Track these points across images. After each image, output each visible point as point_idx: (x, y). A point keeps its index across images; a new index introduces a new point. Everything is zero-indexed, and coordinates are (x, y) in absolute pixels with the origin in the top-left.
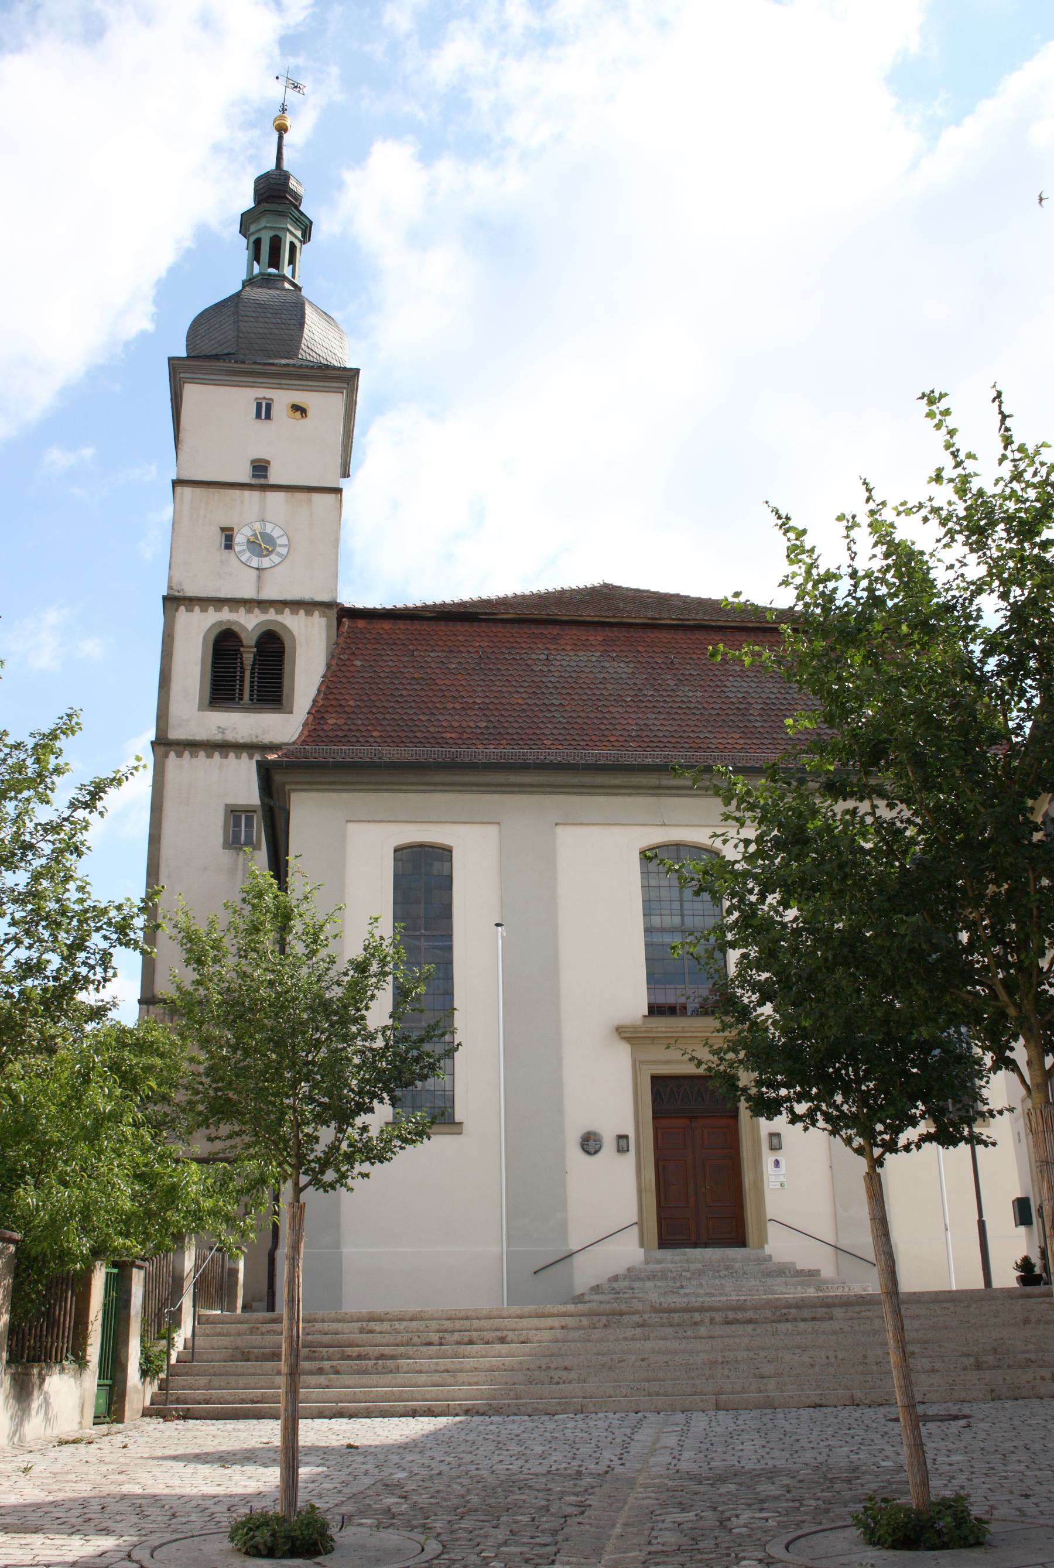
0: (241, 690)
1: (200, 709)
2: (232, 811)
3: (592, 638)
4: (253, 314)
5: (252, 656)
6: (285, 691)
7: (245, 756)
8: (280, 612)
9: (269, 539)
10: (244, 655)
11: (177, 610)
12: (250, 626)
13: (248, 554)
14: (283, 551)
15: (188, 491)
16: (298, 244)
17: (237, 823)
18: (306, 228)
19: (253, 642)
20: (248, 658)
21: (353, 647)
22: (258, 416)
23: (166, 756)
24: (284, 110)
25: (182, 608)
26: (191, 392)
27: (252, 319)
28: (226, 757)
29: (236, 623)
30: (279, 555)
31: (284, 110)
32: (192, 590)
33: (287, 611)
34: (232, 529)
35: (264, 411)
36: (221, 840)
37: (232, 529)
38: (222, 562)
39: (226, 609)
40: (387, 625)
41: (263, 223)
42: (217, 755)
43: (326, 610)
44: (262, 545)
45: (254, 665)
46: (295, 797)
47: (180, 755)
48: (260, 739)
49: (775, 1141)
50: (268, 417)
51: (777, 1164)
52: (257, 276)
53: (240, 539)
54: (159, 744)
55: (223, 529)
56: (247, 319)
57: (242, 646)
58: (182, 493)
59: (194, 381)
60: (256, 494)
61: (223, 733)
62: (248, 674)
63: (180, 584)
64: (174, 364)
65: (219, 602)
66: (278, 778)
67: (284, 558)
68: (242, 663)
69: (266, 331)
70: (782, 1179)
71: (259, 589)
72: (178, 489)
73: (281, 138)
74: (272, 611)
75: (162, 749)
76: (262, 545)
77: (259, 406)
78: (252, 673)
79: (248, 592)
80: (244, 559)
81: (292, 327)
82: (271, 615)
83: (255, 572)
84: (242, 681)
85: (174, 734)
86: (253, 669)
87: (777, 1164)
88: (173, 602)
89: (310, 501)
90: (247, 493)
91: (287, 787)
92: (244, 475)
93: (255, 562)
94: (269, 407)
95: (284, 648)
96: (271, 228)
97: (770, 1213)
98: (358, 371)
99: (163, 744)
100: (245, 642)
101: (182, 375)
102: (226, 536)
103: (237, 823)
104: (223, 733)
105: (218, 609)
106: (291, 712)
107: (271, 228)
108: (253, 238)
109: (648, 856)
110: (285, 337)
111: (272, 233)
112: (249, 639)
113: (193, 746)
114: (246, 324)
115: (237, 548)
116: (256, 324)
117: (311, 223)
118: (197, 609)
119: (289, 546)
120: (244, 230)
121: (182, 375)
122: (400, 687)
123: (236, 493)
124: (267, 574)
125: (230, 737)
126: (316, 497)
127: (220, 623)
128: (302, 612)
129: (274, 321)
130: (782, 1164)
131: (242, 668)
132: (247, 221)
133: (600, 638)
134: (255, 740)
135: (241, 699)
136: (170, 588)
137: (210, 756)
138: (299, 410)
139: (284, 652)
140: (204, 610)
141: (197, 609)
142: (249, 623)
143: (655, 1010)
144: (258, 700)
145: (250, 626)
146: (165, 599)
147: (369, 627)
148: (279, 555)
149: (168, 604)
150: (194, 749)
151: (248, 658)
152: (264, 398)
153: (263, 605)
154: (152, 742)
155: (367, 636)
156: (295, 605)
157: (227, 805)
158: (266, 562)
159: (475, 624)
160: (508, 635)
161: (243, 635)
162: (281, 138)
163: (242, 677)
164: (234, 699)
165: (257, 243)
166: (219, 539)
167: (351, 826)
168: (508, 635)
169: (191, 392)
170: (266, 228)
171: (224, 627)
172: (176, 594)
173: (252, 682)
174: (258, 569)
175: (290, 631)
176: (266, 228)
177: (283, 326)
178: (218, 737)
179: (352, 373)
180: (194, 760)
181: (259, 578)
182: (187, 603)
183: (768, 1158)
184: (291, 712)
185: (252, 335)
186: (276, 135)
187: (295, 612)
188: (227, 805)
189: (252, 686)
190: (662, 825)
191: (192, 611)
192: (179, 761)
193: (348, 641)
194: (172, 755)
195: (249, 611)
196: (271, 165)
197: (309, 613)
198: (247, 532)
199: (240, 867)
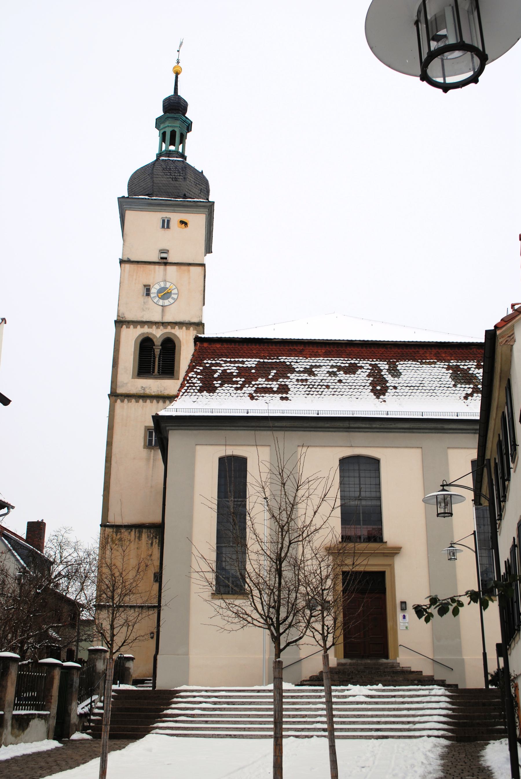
1: (133, 378)
2: (148, 429)
3: (319, 351)
4: (161, 174)
5: (159, 350)
7: (155, 401)
10: (155, 350)
11: (122, 327)
12: (158, 336)
14: (175, 296)
15: (127, 266)
16: (184, 133)
18: (189, 125)
19: (160, 344)
20: (157, 351)
21: (201, 356)
22: (163, 227)
23: (116, 401)
24: (178, 62)
25: (124, 326)
26: (130, 215)
27: (160, 176)
28: (146, 402)
29: (151, 334)
30: (173, 298)
31: (178, 62)
32: (129, 317)
33: (177, 327)
34: (150, 286)
35: (166, 224)
36: (142, 444)
37: (150, 286)
38: (144, 303)
39: (146, 327)
40: (218, 346)
41: (167, 124)
42: (141, 401)
43: (197, 327)
44: (165, 294)
46: (170, 432)
47: (122, 401)
48: (162, 393)
49: (403, 605)
50: (168, 227)
51: (404, 617)
53: (154, 291)
54: (112, 396)
55: (145, 286)
56: (157, 176)
57: (154, 345)
58: (125, 267)
59: (130, 209)
60: (162, 267)
61: (144, 390)
62: (157, 359)
63: (123, 314)
64: (122, 201)
65: (143, 323)
66: (163, 425)
67: (175, 300)
70: (407, 625)
71: (163, 316)
72: (123, 265)
74: (169, 327)
75: (114, 398)
76: (165, 294)
77: (163, 221)
79: (157, 318)
80: (155, 301)
81: (181, 180)
82: (169, 330)
83: (161, 308)
84: (154, 363)
85: (120, 391)
86: (159, 357)
87: (404, 617)
88: (120, 323)
89: (189, 271)
90: (157, 267)
91: (167, 428)
92: (155, 258)
93: (161, 302)
94: (168, 221)
96: (171, 126)
97: (400, 642)
98: (214, 202)
99: (114, 395)
100: (155, 343)
101: (125, 206)
102: (147, 289)
103: (151, 435)
104: (144, 390)
105: (142, 327)
107: (171, 126)
108: (162, 131)
109: (344, 462)
110: (177, 185)
111: (171, 129)
112: (158, 342)
113: (129, 396)
114: (157, 179)
115: (152, 295)
116: (162, 179)
117: (192, 122)
118: (132, 326)
119: (178, 294)
120: (157, 126)
121: (125, 206)
122: (224, 377)
123: (152, 267)
124: (167, 309)
125: (148, 392)
126: (192, 268)
127: (143, 334)
128: (184, 328)
130: (407, 617)
132: (159, 122)
133: (324, 351)
134: (160, 393)
135: (154, 372)
136: (118, 316)
137: (137, 402)
138: (183, 223)
139: (175, 348)
140: (135, 327)
141: (132, 326)
143: (345, 538)
144: (162, 373)
145: (158, 336)
146: (116, 322)
147: (209, 346)
148: (173, 298)
149: (117, 324)
150: (130, 398)
151: (157, 351)
152: (166, 217)
153: (164, 324)
154: (109, 395)
155: (208, 351)
156: (180, 324)
157: (146, 427)
158: (166, 302)
159: (262, 344)
160: (278, 350)
161: (155, 340)
164: (150, 372)
166: (143, 291)
167: (198, 448)
168: (278, 350)
169: (130, 215)
170: (168, 126)
171: (145, 336)
172: (121, 319)
173: (159, 364)
174: (162, 306)
175: (178, 338)
176: (168, 126)
178: (140, 391)
179: (211, 204)
180: (130, 404)
181: (163, 310)
182: (127, 324)
183: (400, 615)
185: (160, 185)
186: (174, 76)
187: (181, 328)
188: (146, 427)
190: (350, 447)
191: (129, 328)
192: (122, 404)
193: (199, 353)
194: (119, 401)
195: (158, 328)
196: (172, 93)
198: (157, 287)
199: (152, 458)
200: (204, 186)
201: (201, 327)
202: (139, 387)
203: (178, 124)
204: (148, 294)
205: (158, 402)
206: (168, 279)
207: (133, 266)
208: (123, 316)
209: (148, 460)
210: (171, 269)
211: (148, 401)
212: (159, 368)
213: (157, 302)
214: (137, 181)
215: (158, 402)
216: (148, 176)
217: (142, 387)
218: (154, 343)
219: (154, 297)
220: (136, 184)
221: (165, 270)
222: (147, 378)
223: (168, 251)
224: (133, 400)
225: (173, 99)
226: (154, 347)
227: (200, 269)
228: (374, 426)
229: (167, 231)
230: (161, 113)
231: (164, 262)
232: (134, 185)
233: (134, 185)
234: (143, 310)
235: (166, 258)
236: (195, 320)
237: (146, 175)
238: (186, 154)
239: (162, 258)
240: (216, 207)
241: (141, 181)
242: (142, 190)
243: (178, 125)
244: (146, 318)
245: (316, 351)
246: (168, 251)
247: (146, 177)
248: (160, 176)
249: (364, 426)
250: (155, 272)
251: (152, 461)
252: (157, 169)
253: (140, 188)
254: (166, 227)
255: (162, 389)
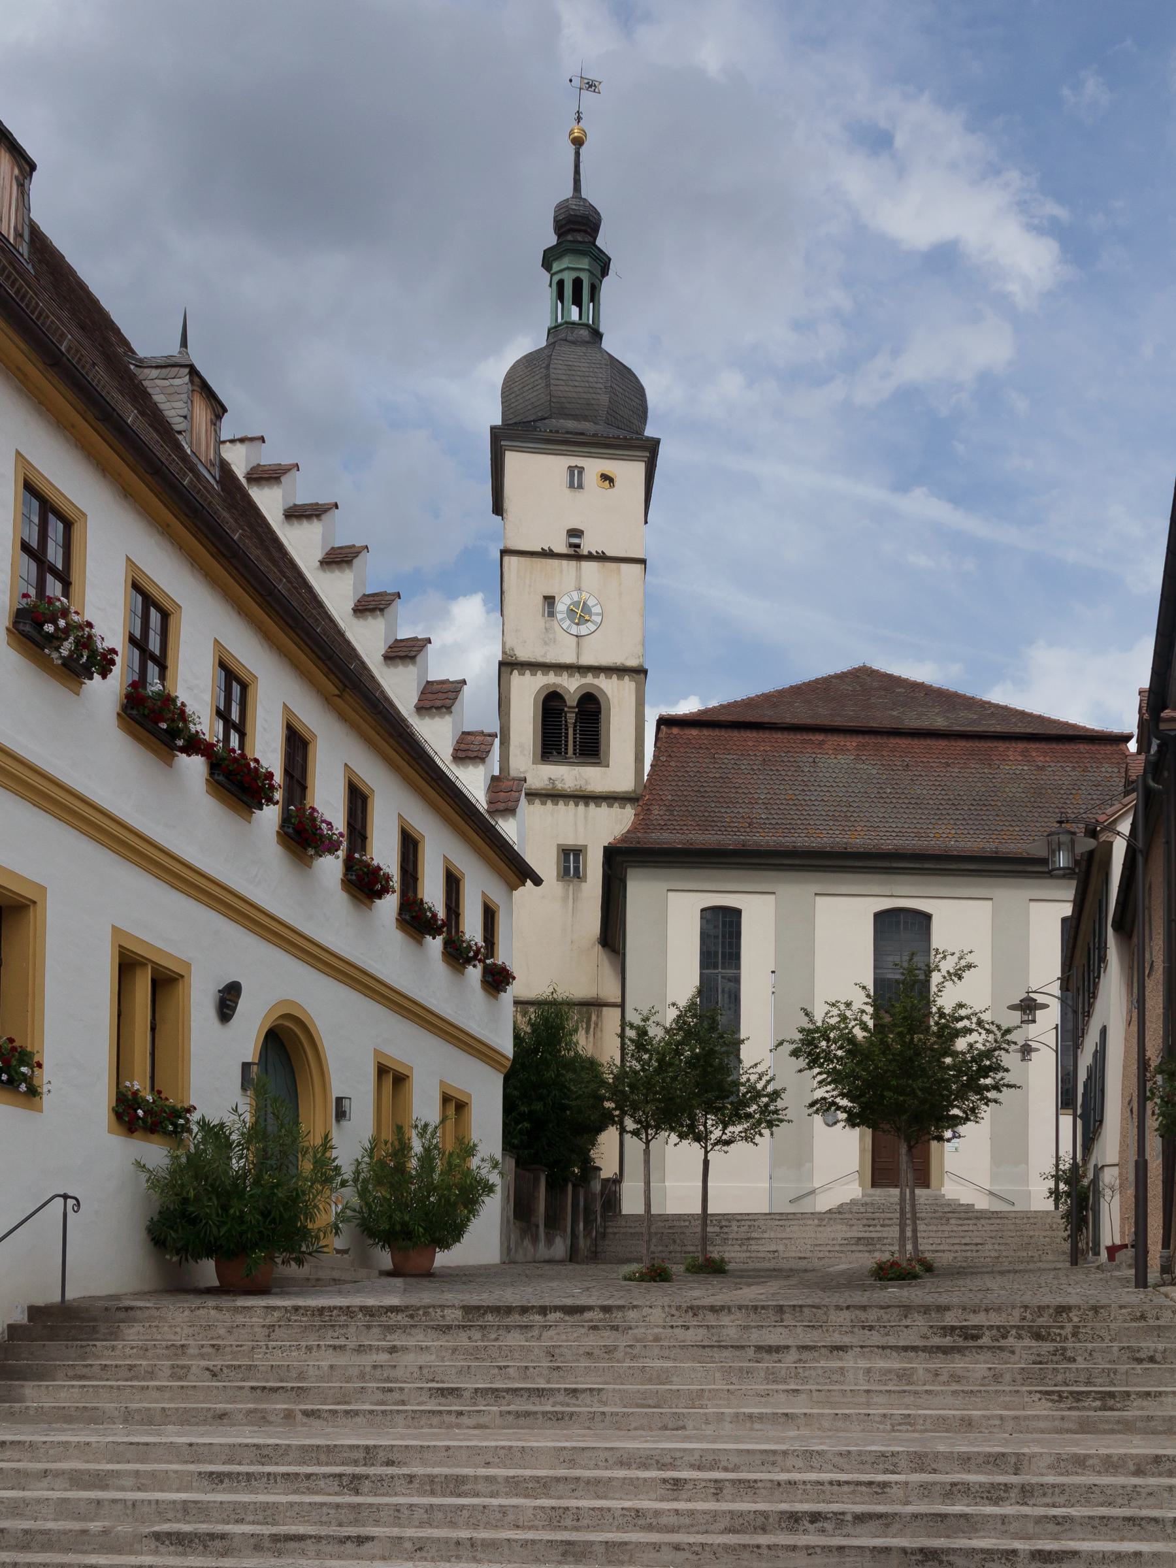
0: (566, 745)
4: (564, 377)
6: (603, 747)
8: (596, 676)
9: (586, 608)
11: (511, 673)
12: (572, 689)
13: (568, 622)
17: (567, 860)
18: (605, 265)
19: (575, 704)
20: (571, 718)
22: (571, 486)
24: (579, 119)
25: (515, 672)
26: (514, 461)
27: (562, 383)
28: (557, 804)
29: (560, 686)
31: (579, 119)
32: (523, 655)
34: (553, 598)
37: (553, 598)
38: (546, 629)
41: (565, 262)
45: (576, 722)
50: (580, 486)
52: (561, 325)
53: (561, 607)
55: (546, 598)
58: (510, 562)
60: (573, 563)
62: (571, 731)
63: (513, 650)
68: (566, 721)
69: (575, 395)
73: (577, 154)
76: (579, 613)
78: (575, 730)
79: (569, 658)
81: (599, 391)
82: (589, 679)
86: (575, 727)
89: (619, 570)
90: (565, 562)
93: (574, 630)
95: (600, 708)
100: (569, 703)
101: (502, 443)
103: (567, 860)
105: (545, 674)
106: (608, 766)
108: (556, 279)
110: (593, 402)
111: (574, 275)
114: (556, 388)
115: (559, 616)
119: (602, 614)
120: (547, 264)
121: (502, 443)
123: (555, 562)
124: (584, 641)
127: (547, 686)
129: (582, 384)
131: (566, 726)
132: (549, 259)
135: (566, 753)
136: (504, 652)
137: (543, 803)
138: (607, 478)
139: (599, 712)
140: (534, 674)
142: (571, 685)
145: (572, 689)
158: (583, 630)
161: (566, 697)
162: (577, 154)
163: (567, 734)
165: (561, 284)
169: (514, 461)
173: (575, 738)
174: (577, 636)
175: (605, 694)
176: (568, 268)
177: (591, 390)
180: (531, 807)
181: (578, 644)
184: (608, 766)
186: (571, 149)
187: (609, 677)
189: (575, 742)
191: (524, 675)
195: (571, 675)
196: (568, 192)
197: (620, 678)
200: (636, 400)
201: (642, 676)
202: (546, 778)
203: (584, 263)
204: (552, 614)
205: (577, 805)
206: (584, 586)
207: (522, 559)
208: (512, 653)
209: (565, 898)
210: (589, 567)
211: (561, 803)
212: (575, 746)
213: (568, 628)
214: (520, 387)
215: (577, 805)
216: (540, 381)
217: (550, 779)
218: (565, 702)
219: (562, 619)
220: (518, 393)
221: (579, 570)
222: (556, 763)
223: (582, 532)
224: (537, 801)
225: (574, 207)
226: (566, 709)
227: (638, 568)
228: (926, 866)
229: (579, 495)
230: (552, 240)
231: (576, 555)
232: (514, 395)
233: (514, 395)
234: (546, 643)
235: (578, 546)
236: (632, 663)
237: (537, 377)
238: (602, 330)
239: (571, 545)
240: (663, 450)
241: (527, 388)
242: (530, 407)
243: (587, 267)
244: (550, 659)
245: (842, 743)
246: (582, 532)
247: (537, 383)
248: (562, 383)
249: (912, 865)
250: (561, 572)
251: (571, 901)
252: (555, 366)
253: (527, 403)
254: (576, 486)
255: (582, 783)
